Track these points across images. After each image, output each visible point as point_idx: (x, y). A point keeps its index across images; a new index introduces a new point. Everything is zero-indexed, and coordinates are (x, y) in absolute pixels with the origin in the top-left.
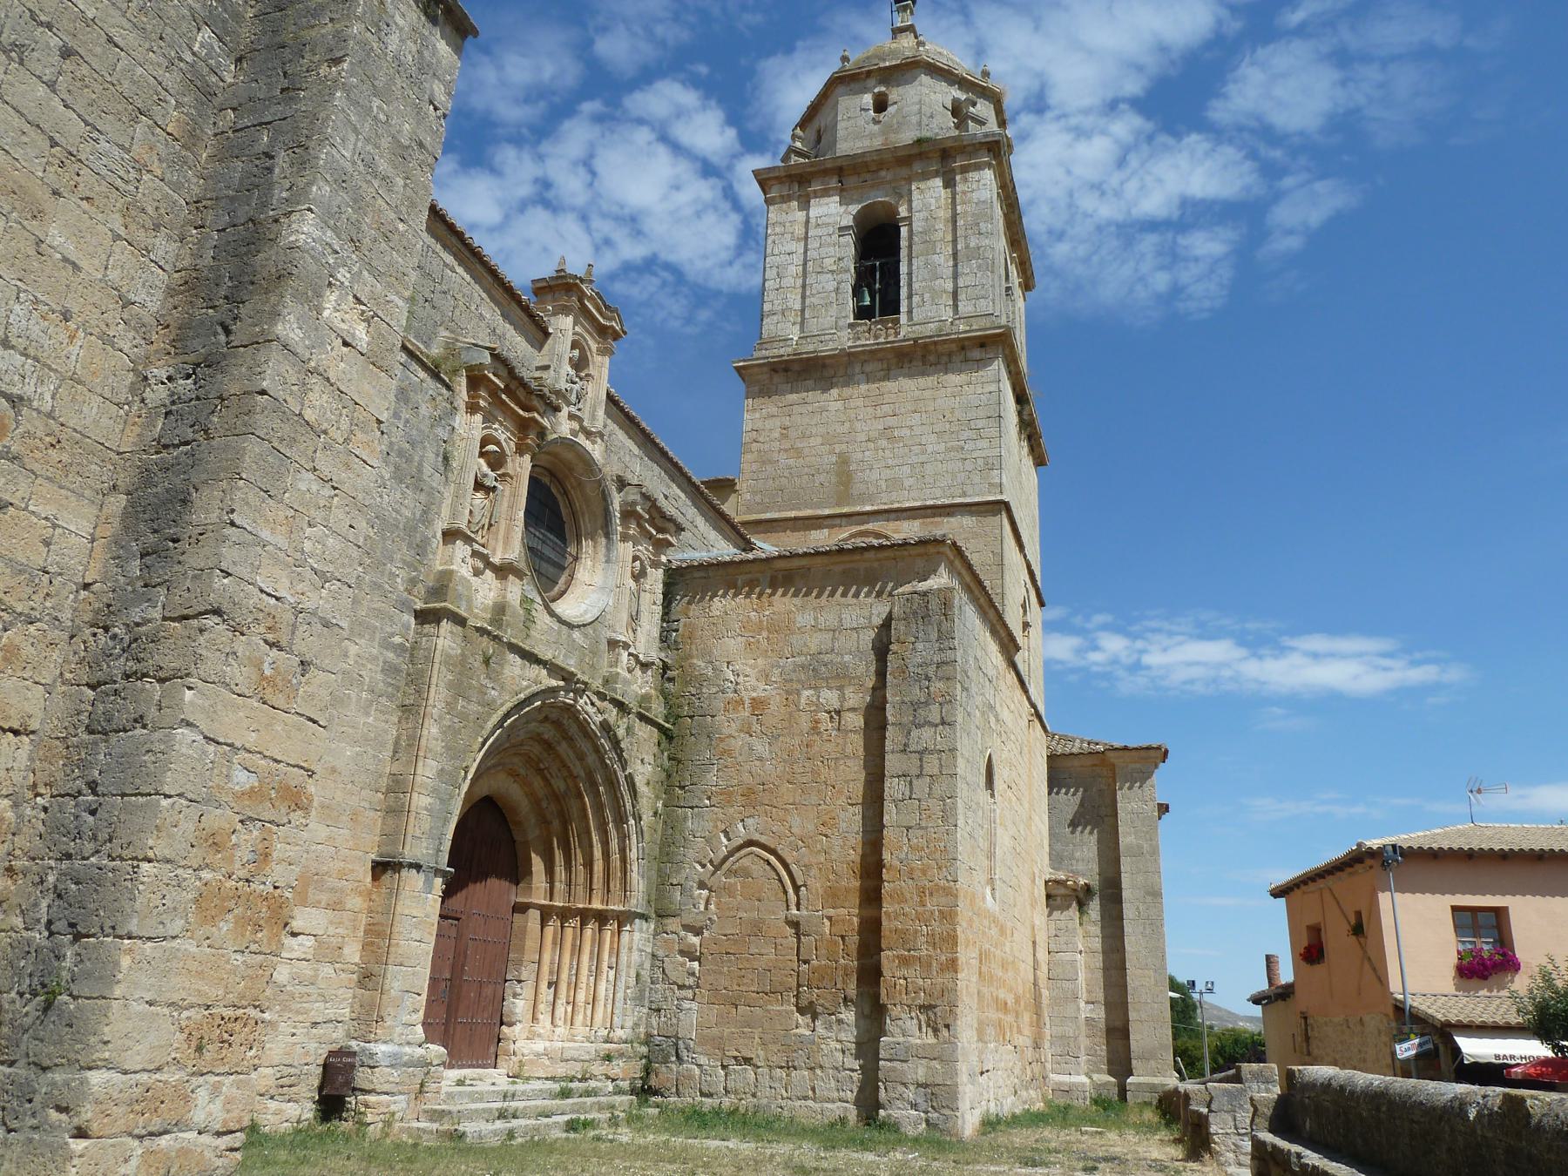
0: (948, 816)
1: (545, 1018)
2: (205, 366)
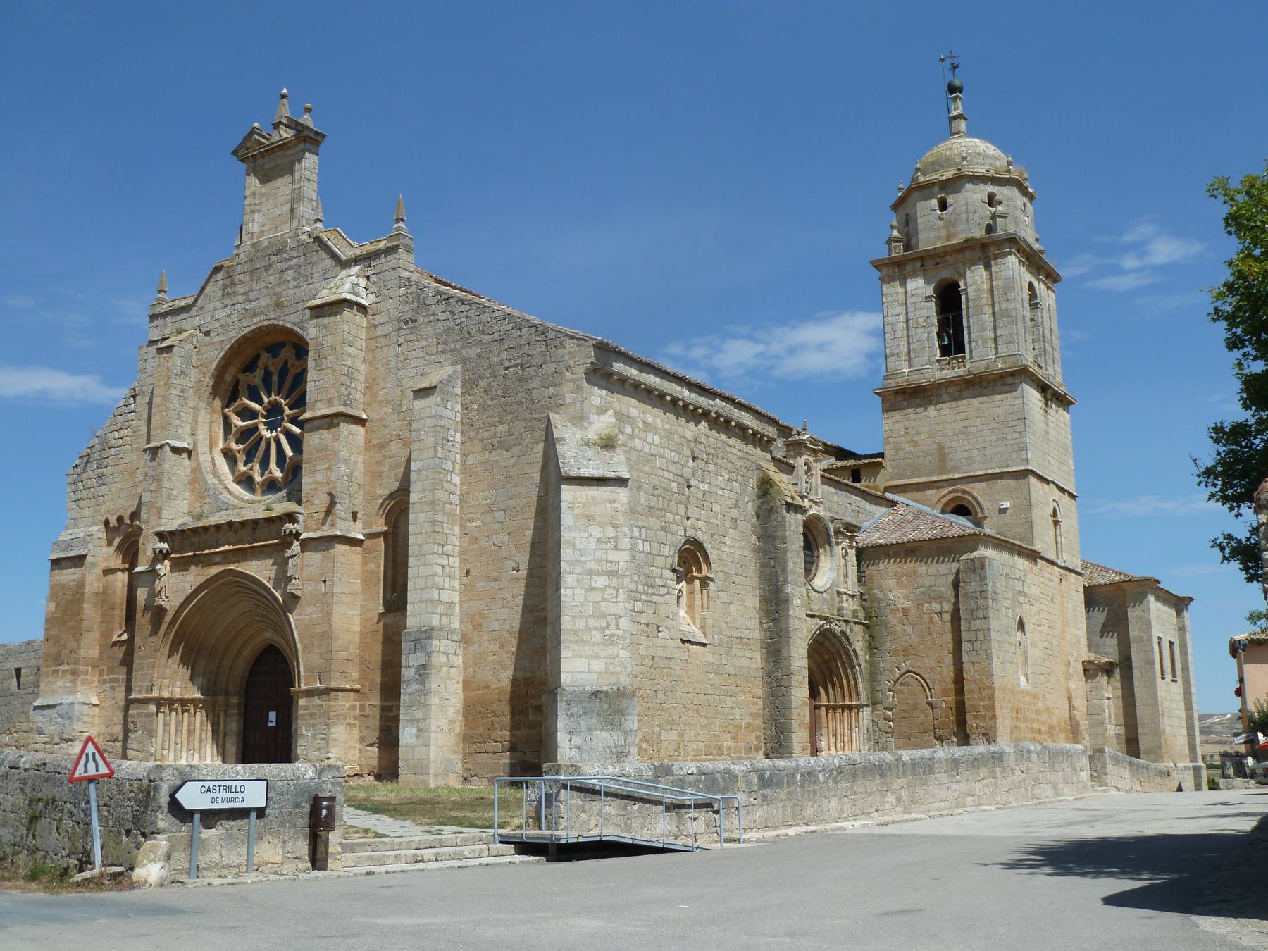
0: (989, 657)
1: (833, 749)
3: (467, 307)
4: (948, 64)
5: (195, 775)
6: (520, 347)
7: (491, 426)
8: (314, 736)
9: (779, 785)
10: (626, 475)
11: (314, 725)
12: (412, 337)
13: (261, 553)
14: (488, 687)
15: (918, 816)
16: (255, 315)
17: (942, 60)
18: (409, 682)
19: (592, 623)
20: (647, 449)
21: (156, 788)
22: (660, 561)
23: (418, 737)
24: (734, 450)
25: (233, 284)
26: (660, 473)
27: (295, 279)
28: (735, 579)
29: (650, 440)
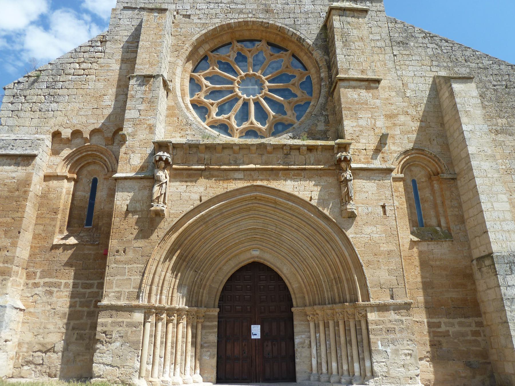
8: (396, 352)
13: (299, 175)
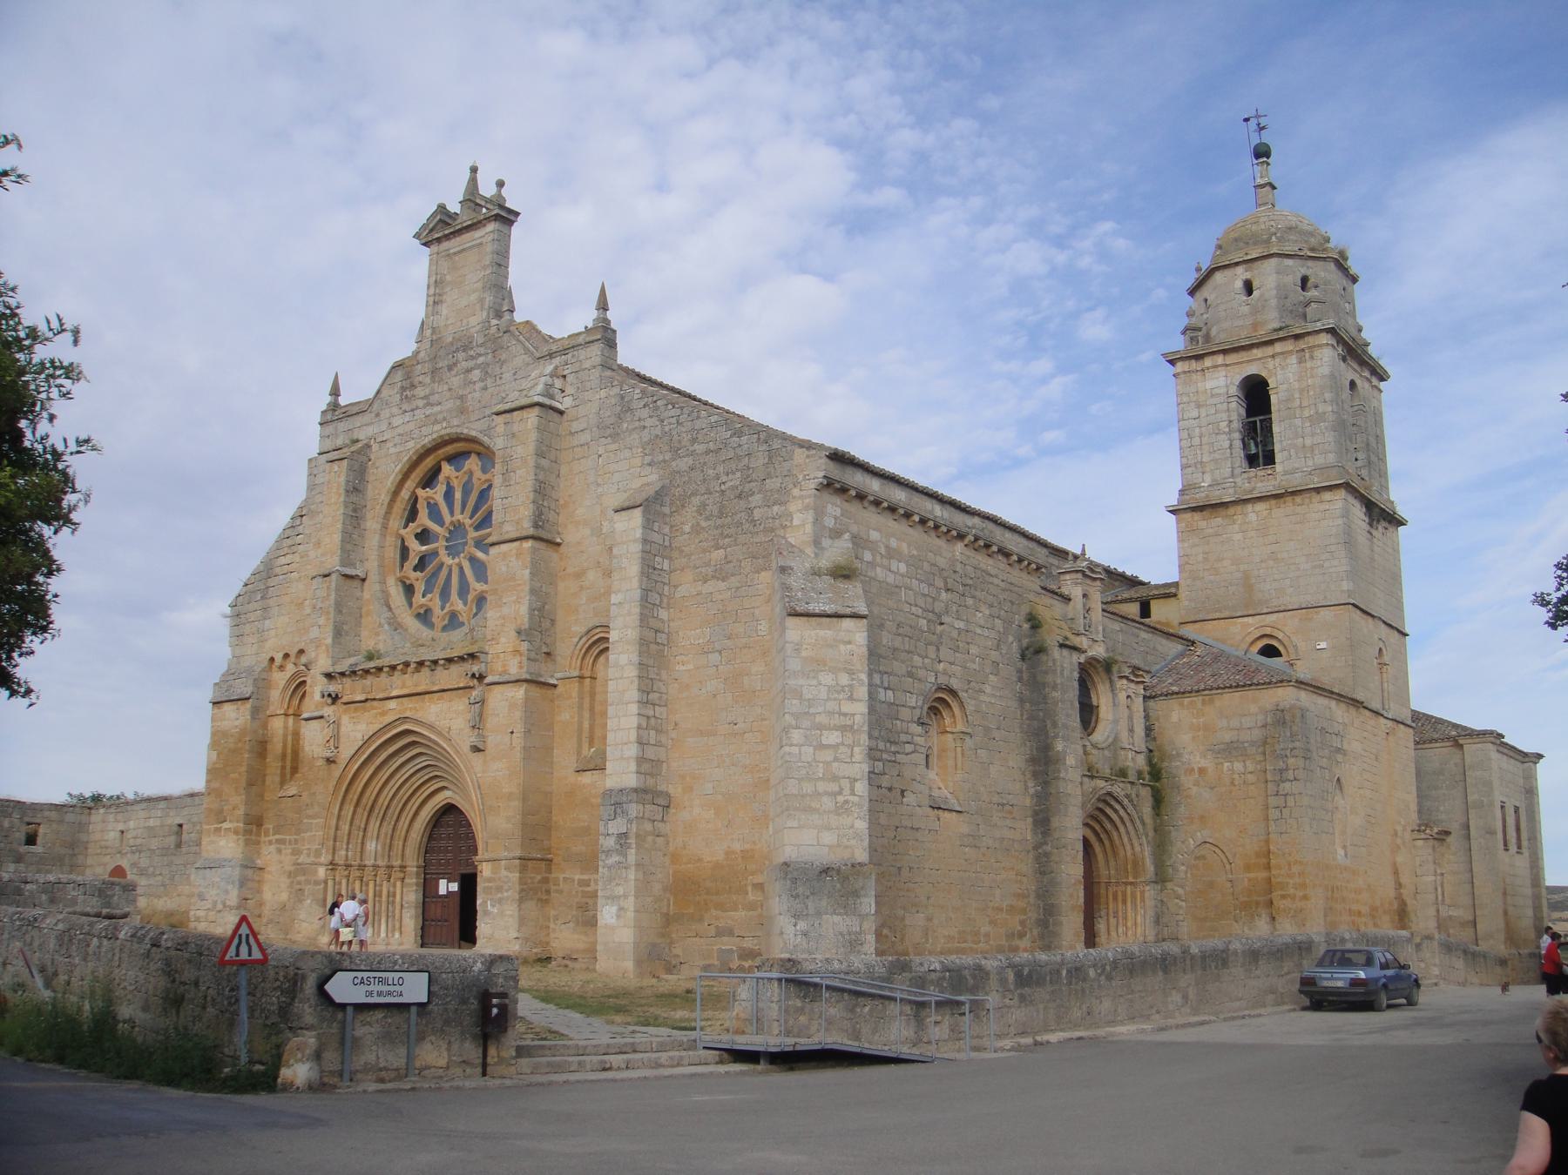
2: (1046, 784)
3: (678, 412)
4: (1253, 123)
5: (346, 964)
6: (739, 458)
7: (704, 551)
9: (1040, 982)
10: (863, 610)
11: (500, 901)
12: (613, 447)
14: (700, 860)
15: (1206, 1018)
16: (436, 422)
17: (1246, 120)
18: (608, 853)
19: (821, 787)
20: (891, 579)
21: (304, 977)
22: (905, 713)
23: (618, 917)
24: (996, 581)
25: (413, 386)
26: (906, 608)
27: (482, 380)
28: (996, 734)
29: (894, 568)
